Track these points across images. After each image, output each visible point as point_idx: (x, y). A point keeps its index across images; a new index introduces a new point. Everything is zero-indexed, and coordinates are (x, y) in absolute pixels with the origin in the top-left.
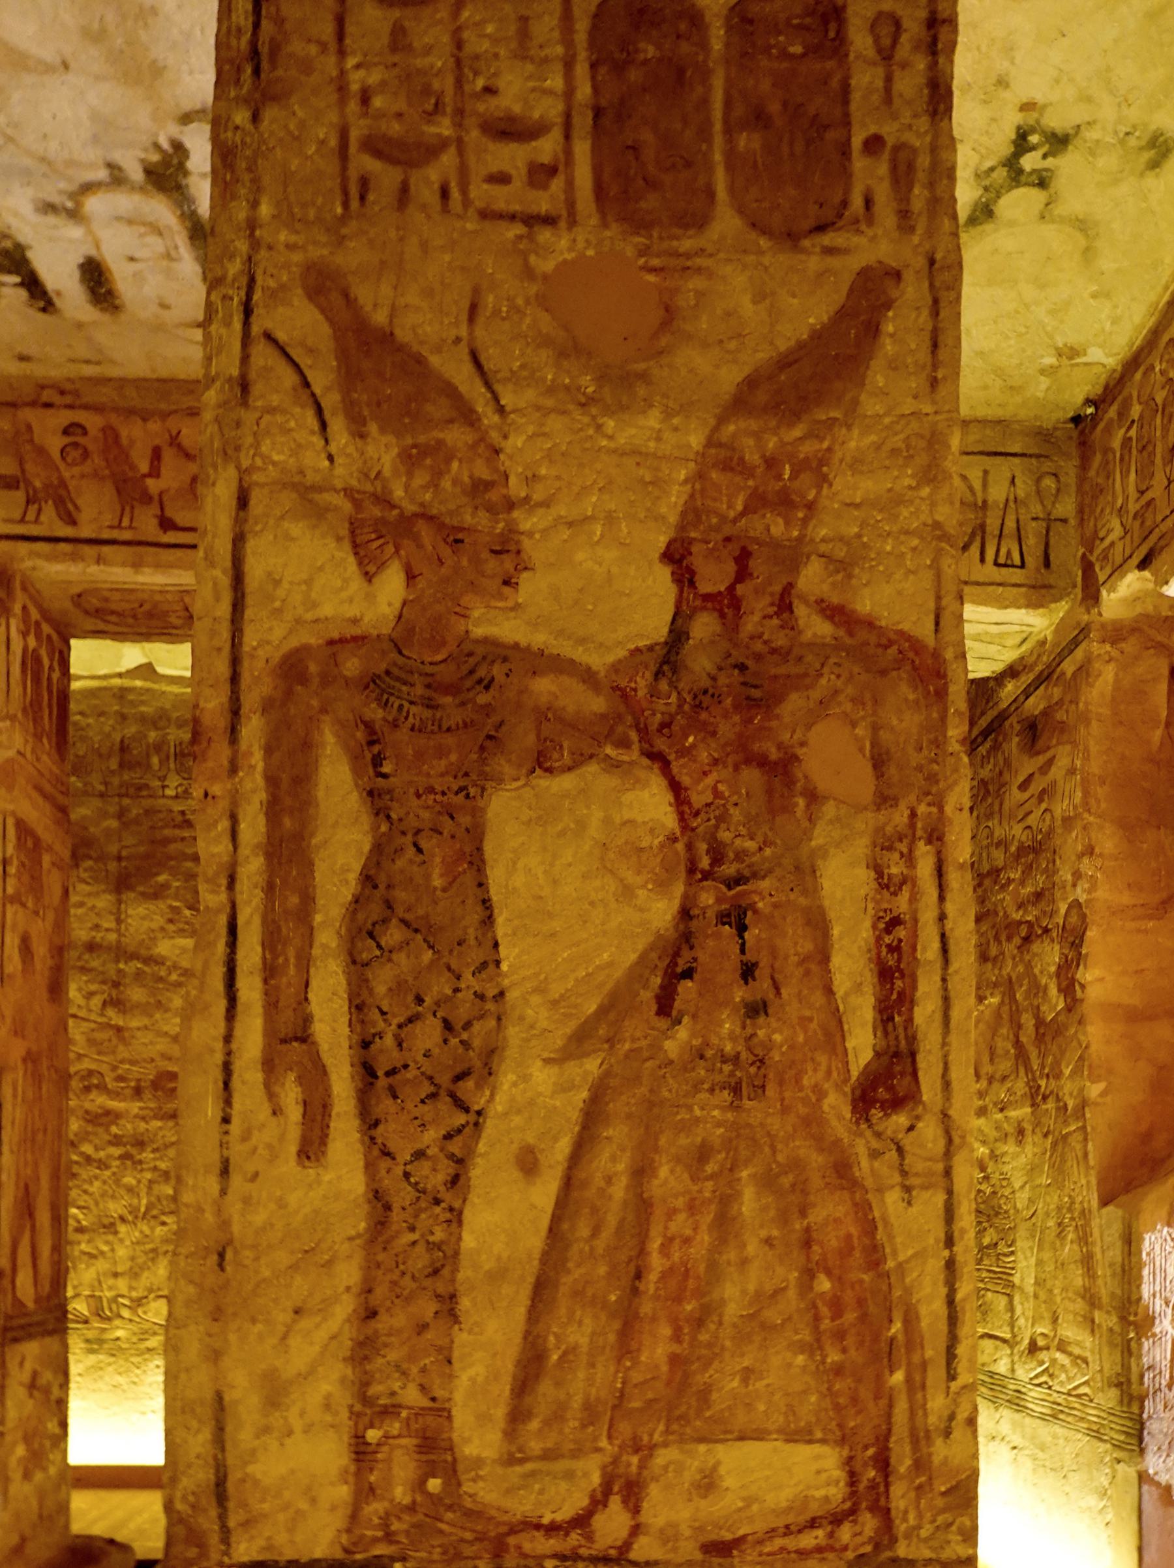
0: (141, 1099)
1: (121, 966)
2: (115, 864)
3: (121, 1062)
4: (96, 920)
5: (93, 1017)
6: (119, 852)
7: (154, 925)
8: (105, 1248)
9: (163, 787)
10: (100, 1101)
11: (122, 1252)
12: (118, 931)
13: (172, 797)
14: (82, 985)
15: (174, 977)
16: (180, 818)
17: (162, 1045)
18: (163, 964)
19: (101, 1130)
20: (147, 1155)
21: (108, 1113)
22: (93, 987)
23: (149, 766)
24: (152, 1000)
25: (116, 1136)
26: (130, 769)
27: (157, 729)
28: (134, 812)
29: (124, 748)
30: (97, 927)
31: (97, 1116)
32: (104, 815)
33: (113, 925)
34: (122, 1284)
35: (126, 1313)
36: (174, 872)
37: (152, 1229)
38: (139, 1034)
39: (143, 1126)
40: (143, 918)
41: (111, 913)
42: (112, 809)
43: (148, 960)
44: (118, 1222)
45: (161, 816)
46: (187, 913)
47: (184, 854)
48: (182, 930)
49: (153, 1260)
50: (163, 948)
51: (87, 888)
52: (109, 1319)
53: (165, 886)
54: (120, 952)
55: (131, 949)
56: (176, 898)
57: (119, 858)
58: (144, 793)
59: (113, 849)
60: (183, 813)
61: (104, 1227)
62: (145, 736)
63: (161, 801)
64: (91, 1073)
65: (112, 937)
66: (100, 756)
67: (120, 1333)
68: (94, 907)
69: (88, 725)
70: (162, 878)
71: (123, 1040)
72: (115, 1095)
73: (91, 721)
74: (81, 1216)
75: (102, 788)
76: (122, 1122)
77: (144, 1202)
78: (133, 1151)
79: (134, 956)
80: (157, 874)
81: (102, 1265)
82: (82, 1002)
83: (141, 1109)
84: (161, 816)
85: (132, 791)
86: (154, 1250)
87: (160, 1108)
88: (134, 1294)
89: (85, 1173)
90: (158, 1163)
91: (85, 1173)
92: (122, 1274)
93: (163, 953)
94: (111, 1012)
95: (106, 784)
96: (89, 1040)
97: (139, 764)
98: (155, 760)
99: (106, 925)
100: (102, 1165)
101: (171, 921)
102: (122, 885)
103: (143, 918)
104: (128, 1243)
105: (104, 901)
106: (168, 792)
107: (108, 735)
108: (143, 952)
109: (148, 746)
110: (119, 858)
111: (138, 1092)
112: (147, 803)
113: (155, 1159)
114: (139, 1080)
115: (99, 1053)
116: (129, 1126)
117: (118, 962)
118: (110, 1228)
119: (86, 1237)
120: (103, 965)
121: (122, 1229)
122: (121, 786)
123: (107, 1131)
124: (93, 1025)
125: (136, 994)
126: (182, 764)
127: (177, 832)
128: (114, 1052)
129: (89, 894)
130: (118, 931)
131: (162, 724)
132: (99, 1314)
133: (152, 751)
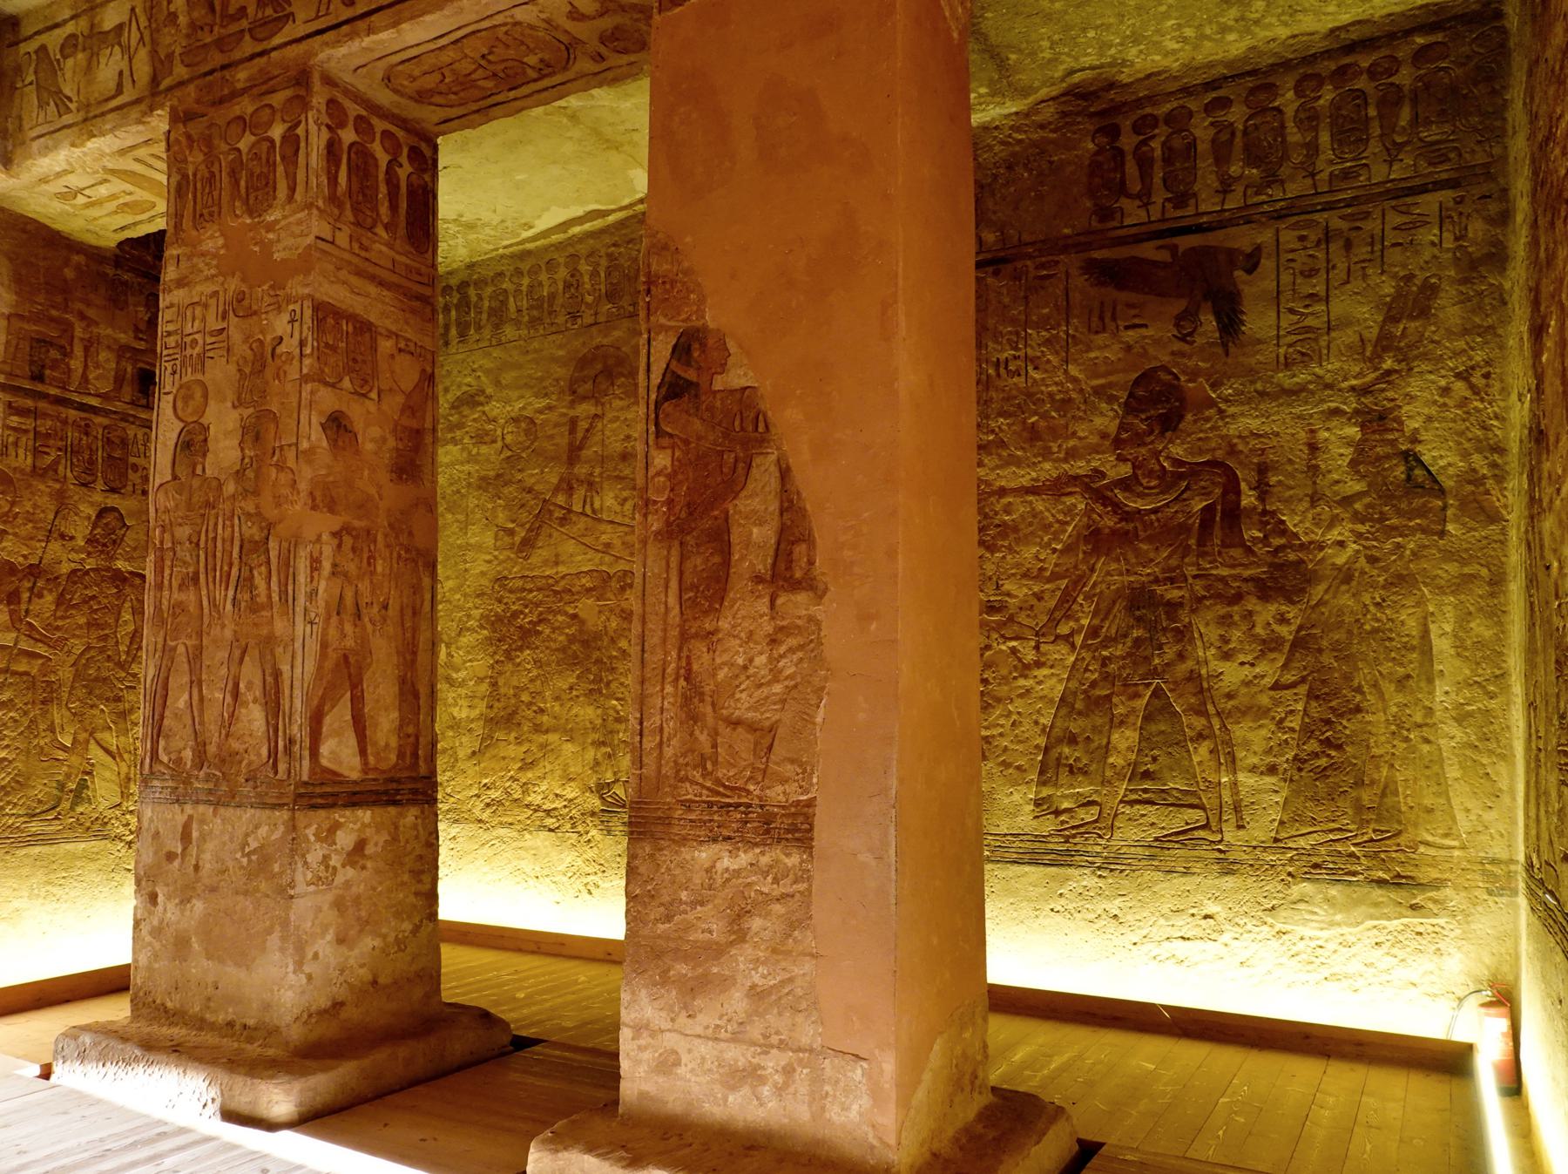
4: (627, 431)
22: (625, 494)
30: (628, 437)
82: (618, 508)
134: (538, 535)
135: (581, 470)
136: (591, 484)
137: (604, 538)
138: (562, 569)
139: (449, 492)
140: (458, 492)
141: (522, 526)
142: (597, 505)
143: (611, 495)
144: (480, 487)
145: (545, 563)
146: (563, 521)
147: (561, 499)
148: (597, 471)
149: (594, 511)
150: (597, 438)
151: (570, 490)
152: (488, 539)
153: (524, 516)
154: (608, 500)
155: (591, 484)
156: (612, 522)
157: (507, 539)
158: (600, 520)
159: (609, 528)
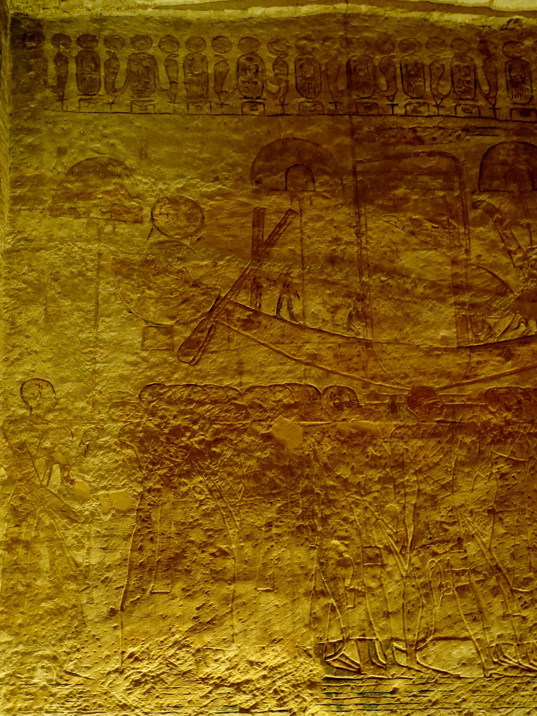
0: (397, 418)
1: (364, 279)
2: (351, 178)
3: (373, 378)
5: (340, 331)
6: (354, 168)
7: (395, 238)
8: (373, 584)
9: (393, 106)
10: (352, 420)
11: (392, 588)
12: (359, 244)
13: (402, 116)
14: (326, 298)
15: (420, 290)
16: (411, 135)
17: (415, 360)
18: (408, 277)
19: (357, 451)
20: (410, 478)
21: (362, 433)
22: (338, 301)
23: (377, 86)
24: (399, 314)
25: (374, 458)
26: (358, 89)
27: (382, 52)
28: (366, 129)
29: (350, 70)
30: (337, 240)
31: (351, 436)
32: (337, 132)
33: (354, 238)
34: (395, 626)
35: (402, 660)
36: (412, 185)
37: (423, 560)
38: (390, 348)
39: (401, 445)
40: (384, 231)
41: (350, 226)
42: (343, 128)
43: (391, 273)
44: (384, 553)
45: (393, 133)
46: (428, 225)
47: (419, 168)
48: (426, 243)
49: (427, 595)
50: (407, 260)
51: (325, 202)
52: (384, 667)
53: (405, 199)
54: (363, 266)
55: (373, 262)
56: (415, 210)
57: (355, 173)
58: (374, 112)
59: (349, 163)
60: (414, 130)
61: (370, 559)
62: (372, 59)
63: (393, 119)
64: (341, 391)
65: (354, 250)
66: (328, 77)
67: (397, 684)
68: (332, 220)
69: (314, 49)
70: (400, 192)
71: (372, 354)
72: (367, 413)
73: (317, 45)
74: (342, 548)
75: (332, 107)
76: (380, 441)
77: (411, 530)
78: (395, 474)
79: (377, 269)
80: (396, 188)
81: (370, 604)
82: (328, 317)
83: (399, 428)
84: (393, 133)
85: (362, 110)
86: (425, 585)
87: (419, 427)
88: (410, 637)
89: (344, 499)
90: (422, 486)
91: (344, 499)
92: (395, 613)
93: (406, 266)
94: (358, 326)
95: (336, 103)
96: (336, 356)
97: (366, 84)
98: (383, 81)
99: (346, 238)
100: (362, 489)
101: (412, 233)
102: (359, 198)
103: (384, 231)
104: (397, 577)
105: (343, 215)
106: (399, 111)
107: (336, 58)
108: (386, 264)
109: (374, 67)
110: (355, 173)
111: (393, 408)
112: (377, 121)
113: (417, 482)
114: (393, 397)
115: (349, 369)
116: (386, 446)
117: (361, 274)
118: (375, 560)
119: (350, 571)
120: (346, 278)
121: (390, 561)
122: (350, 105)
123: (364, 452)
124: (340, 341)
125: (383, 307)
126: (410, 85)
127: (410, 148)
128: (364, 368)
129: (327, 208)
130: (359, 244)
131: (387, 47)
132: (371, 660)
133: (379, 73)
134: (210, 337)
135: (272, 268)
136: (287, 286)
137: (309, 348)
138: (248, 380)
139: (65, 272)
140: (81, 274)
141: (186, 324)
142: (297, 309)
143: (318, 300)
144: (117, 273)
145: (223, 371)
146: (247, 324)
147: (243, 298)
148: (296, 271)
149: (292, 316)
150: (296, 235)
151: (257, 289)
152: (133, 335)
153: (188, 312)
154: (314, 305)
155: (287, 286)
156: (320, 331)
157: (162, 338)
158: (303, 328)
159: (315, 337)
